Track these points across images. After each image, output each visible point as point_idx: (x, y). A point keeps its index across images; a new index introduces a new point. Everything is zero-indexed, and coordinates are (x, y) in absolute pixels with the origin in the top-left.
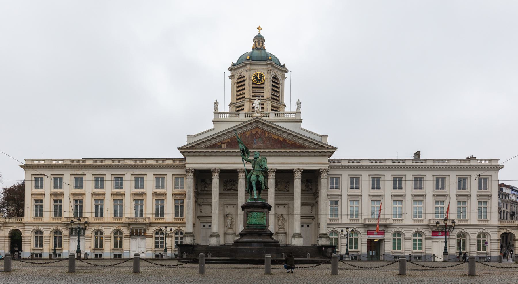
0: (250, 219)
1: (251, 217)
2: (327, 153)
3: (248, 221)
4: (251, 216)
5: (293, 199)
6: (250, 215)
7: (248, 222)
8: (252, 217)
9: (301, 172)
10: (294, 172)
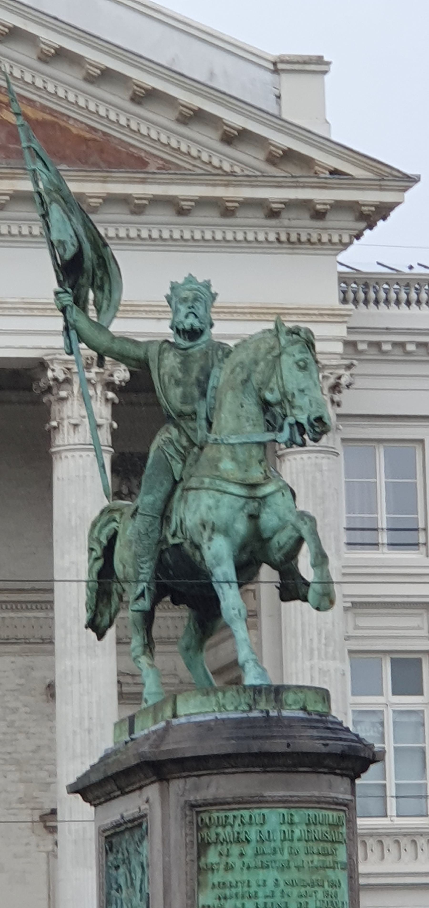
0: (229, 868)
1: (235, 850)
2: (331, 221)
4: (238, 841)
5: (51, 641)
6: (224, 833)
8: (249, 850)
9: (110, 385)
10: (49, 390)
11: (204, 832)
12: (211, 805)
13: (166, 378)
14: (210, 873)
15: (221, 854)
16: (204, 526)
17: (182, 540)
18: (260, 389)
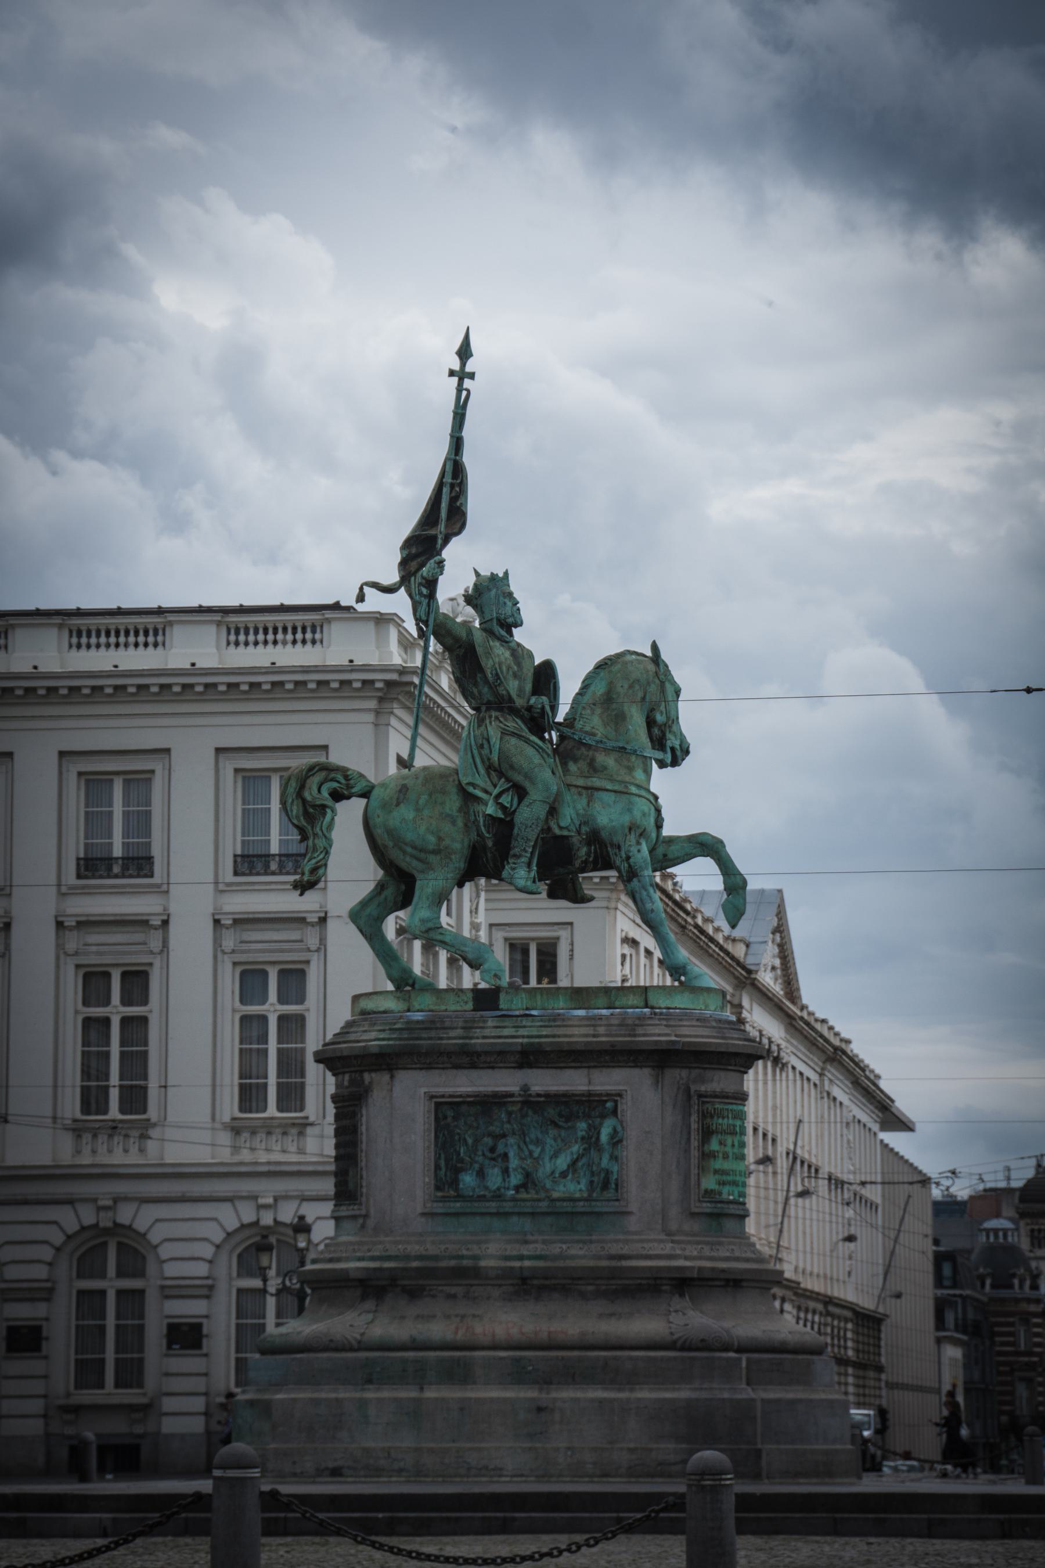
0: (726, 1157)
3: (716, 1172)
7: (709, 1182)
11: (708, 1120)
12: (716, 1097)
13: (504, 668)
14: (712, 1159)
15: (721, 1143)
16: (630, 829)
17: (573, 834)
18: (652, 710)
